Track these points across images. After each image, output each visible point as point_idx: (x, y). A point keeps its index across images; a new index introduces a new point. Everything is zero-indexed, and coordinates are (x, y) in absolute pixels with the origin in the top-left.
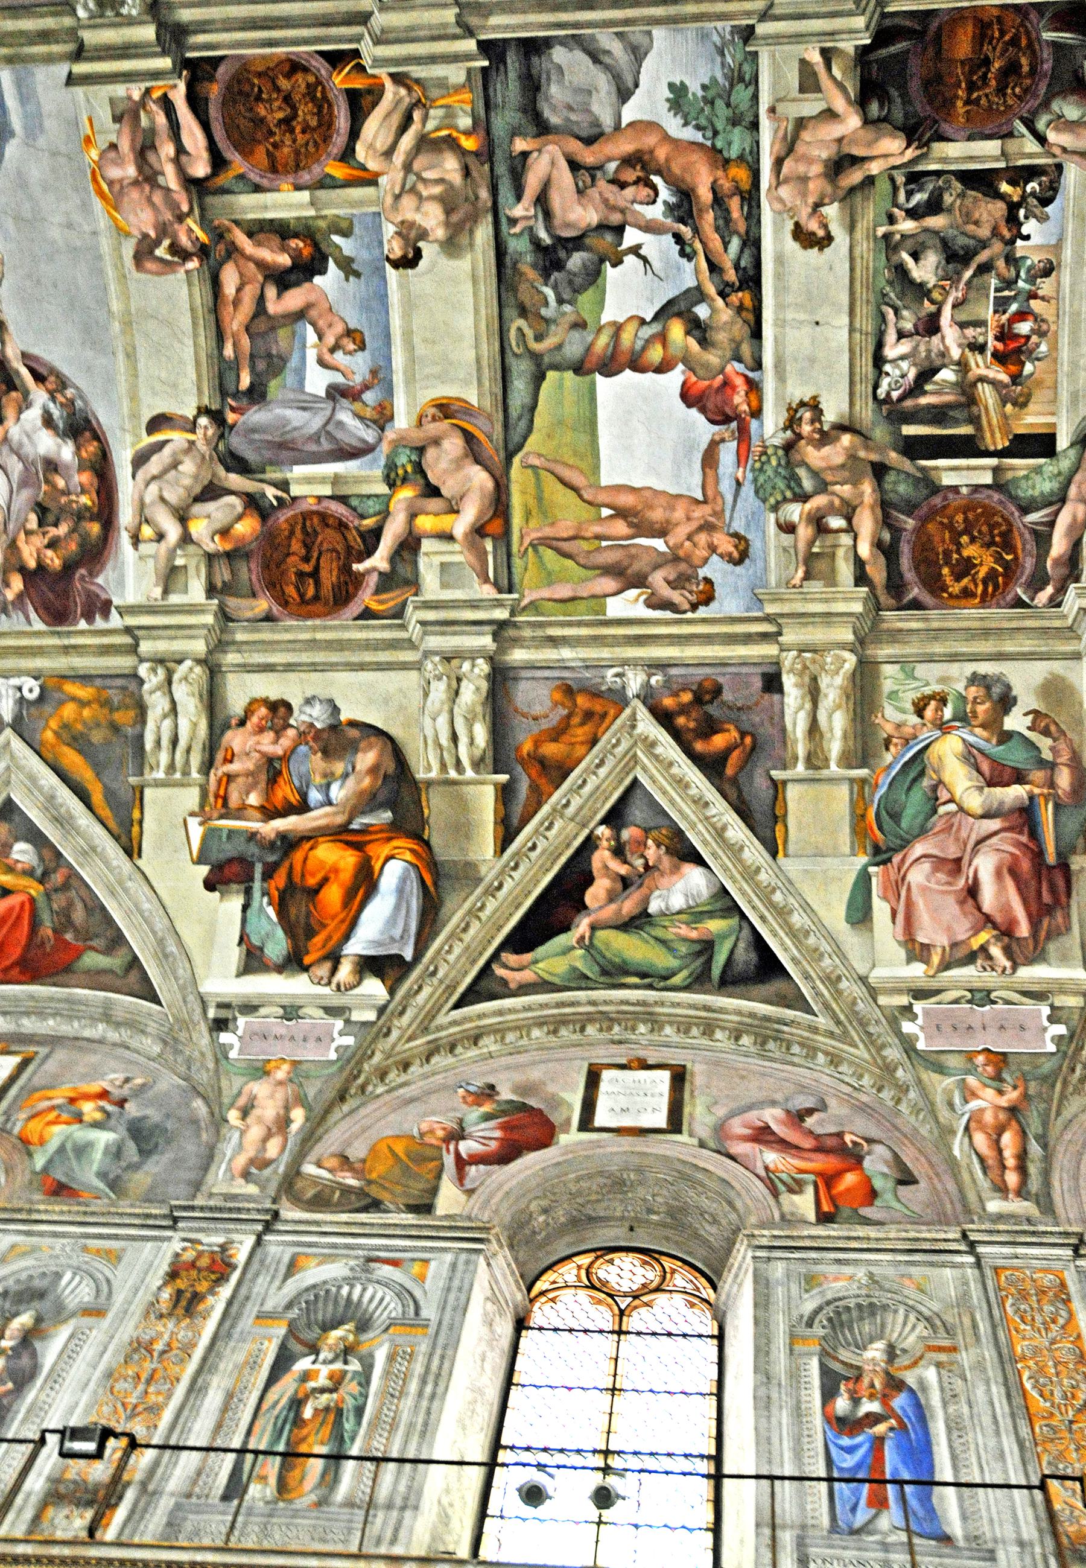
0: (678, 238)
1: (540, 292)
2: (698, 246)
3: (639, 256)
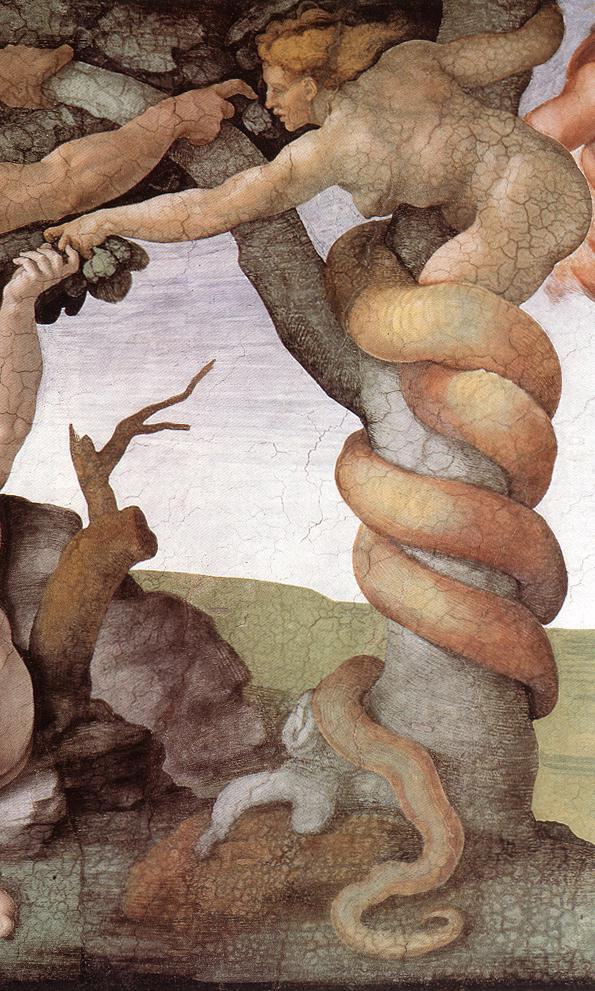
0: (54, 303)
1: (236, 824)
2: (88, 227)
3: (116, 449)
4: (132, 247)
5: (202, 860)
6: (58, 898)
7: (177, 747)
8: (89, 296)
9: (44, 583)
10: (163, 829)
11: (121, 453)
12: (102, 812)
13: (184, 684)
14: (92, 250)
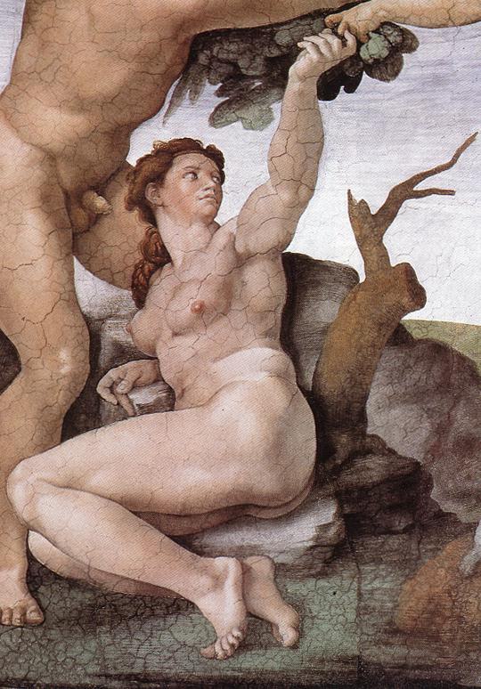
0: (335, 81)
4: (403, 32)
5: (466, 578)
6: (338, 611)
7: (443, 477)
8: (365, 76)
9: (324, 331)
10: (431, 550)
11: (394, 215)
12: (377, 535)
13: (450, 421)
14: (367, 34)
